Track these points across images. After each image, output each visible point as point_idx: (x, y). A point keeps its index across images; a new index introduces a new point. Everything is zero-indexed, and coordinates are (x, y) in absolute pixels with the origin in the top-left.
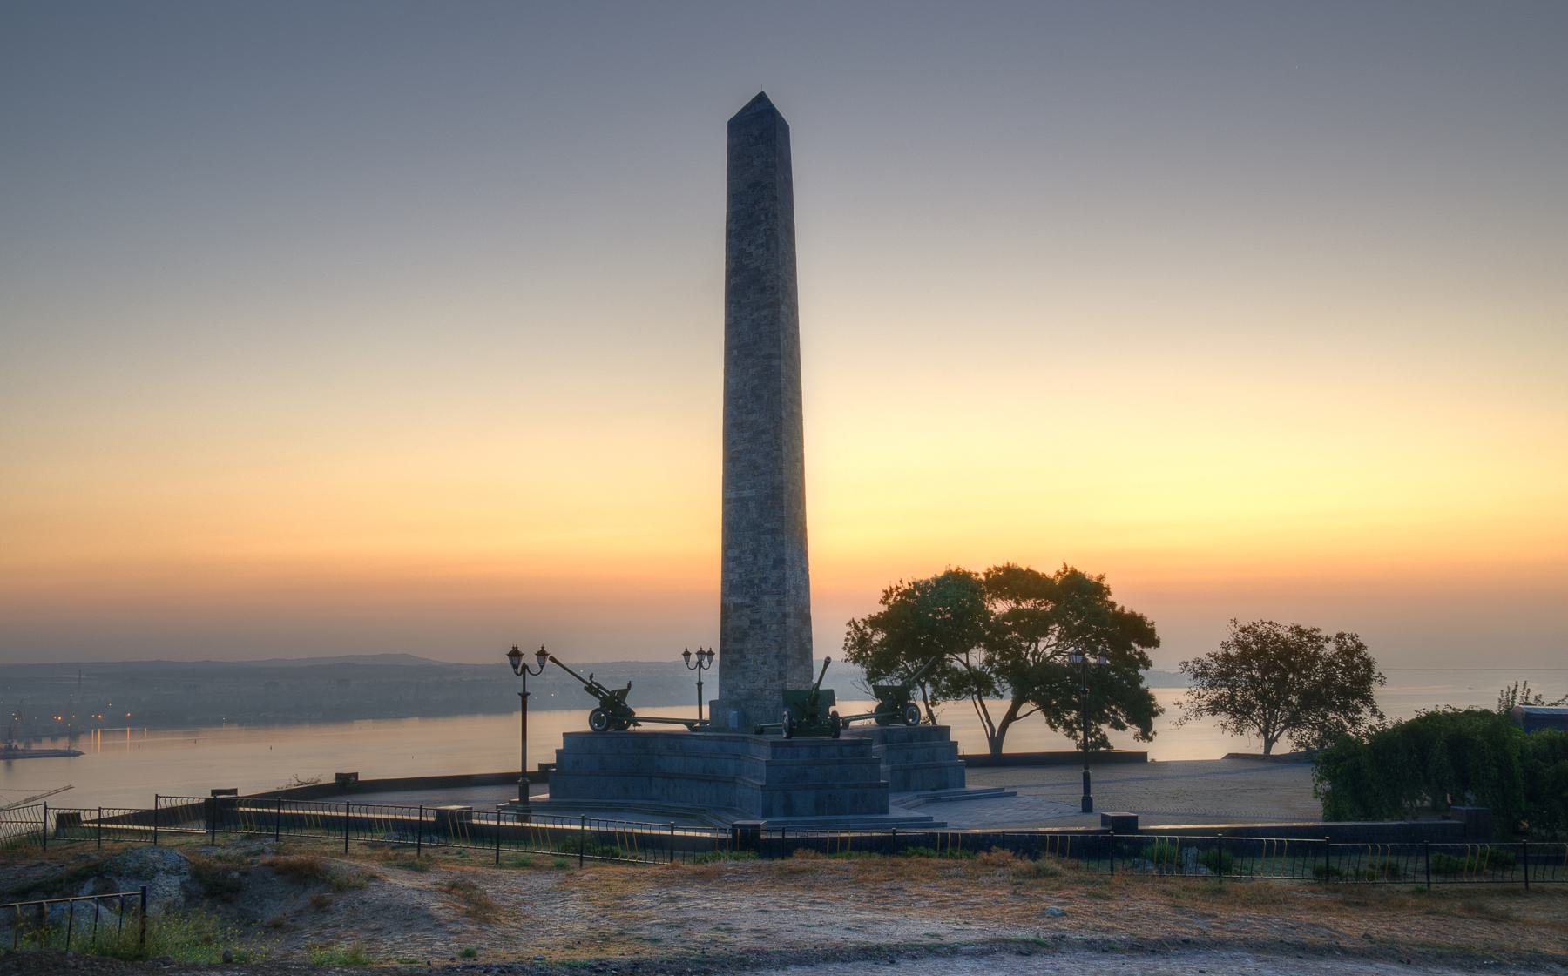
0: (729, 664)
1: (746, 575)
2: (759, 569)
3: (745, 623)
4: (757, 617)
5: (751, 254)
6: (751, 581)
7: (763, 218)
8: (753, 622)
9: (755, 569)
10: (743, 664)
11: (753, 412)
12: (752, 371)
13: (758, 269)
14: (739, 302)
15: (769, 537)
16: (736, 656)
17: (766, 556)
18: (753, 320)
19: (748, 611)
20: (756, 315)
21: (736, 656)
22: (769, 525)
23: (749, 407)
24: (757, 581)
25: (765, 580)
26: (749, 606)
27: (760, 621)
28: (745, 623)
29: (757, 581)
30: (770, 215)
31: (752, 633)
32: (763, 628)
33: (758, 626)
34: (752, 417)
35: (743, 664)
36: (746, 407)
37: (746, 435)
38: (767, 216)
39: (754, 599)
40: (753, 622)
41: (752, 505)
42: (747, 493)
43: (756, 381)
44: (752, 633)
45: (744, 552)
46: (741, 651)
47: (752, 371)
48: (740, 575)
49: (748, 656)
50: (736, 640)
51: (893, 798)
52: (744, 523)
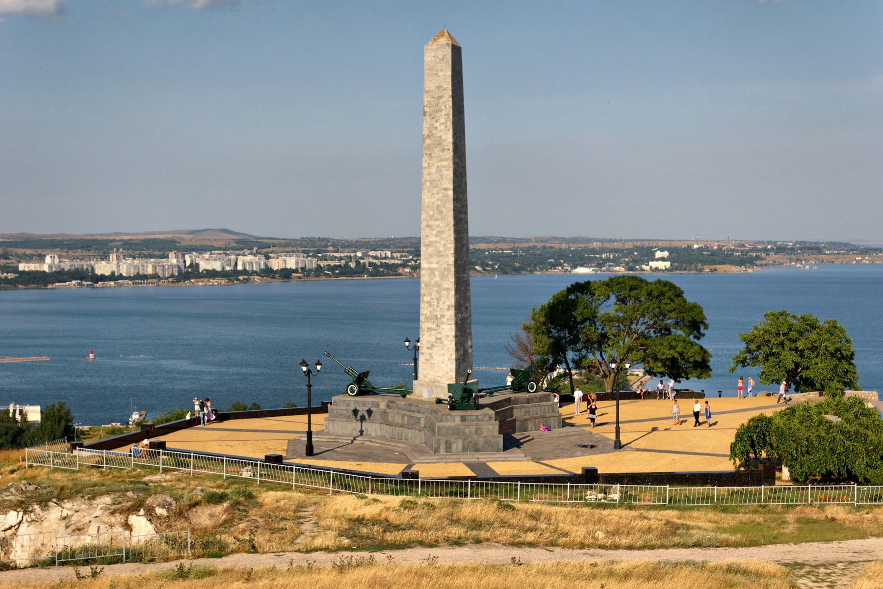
0: (424, 361)
1: (433, 312)
2: (440, 309)
3: (433, 340)
4: (439, 336)
5: (436, 128)
6: (436, 316)
7: (444, 108)
8: (437, 339)
9: (438, 309)
10: (432, 362)
12: (437, 196)
13: (441, 137)
14: (430, 155)
15: (445, 292)
17: (444, 303)
18: (438, 167)
19: (434, 332)
20: (439, 164)
21: (429, 357)
22: (445, 286)
23: (436, 216)
24: (439, 316)
25: (443, 316)
26: (434, 330)
27: (440, 339)
29: (439, 316)
30: (447, 106)
31: (436, 345)
33: (439, 341)
34: (436, 223)
35: (432, 362)
36: (433, 216)
37: (434, 232)
38: (445, 106)
39: (437, 326)
40: (437, 339)
41: (437, 273)
42: (434, 266)
43: (439, 203)
44: (436, 345)
45: (433, 299)
46: (430, 354)
47: (437, 196)
48: (431, 312)
49: (434, 358)
50: (428, 348)
52: (433, 282)
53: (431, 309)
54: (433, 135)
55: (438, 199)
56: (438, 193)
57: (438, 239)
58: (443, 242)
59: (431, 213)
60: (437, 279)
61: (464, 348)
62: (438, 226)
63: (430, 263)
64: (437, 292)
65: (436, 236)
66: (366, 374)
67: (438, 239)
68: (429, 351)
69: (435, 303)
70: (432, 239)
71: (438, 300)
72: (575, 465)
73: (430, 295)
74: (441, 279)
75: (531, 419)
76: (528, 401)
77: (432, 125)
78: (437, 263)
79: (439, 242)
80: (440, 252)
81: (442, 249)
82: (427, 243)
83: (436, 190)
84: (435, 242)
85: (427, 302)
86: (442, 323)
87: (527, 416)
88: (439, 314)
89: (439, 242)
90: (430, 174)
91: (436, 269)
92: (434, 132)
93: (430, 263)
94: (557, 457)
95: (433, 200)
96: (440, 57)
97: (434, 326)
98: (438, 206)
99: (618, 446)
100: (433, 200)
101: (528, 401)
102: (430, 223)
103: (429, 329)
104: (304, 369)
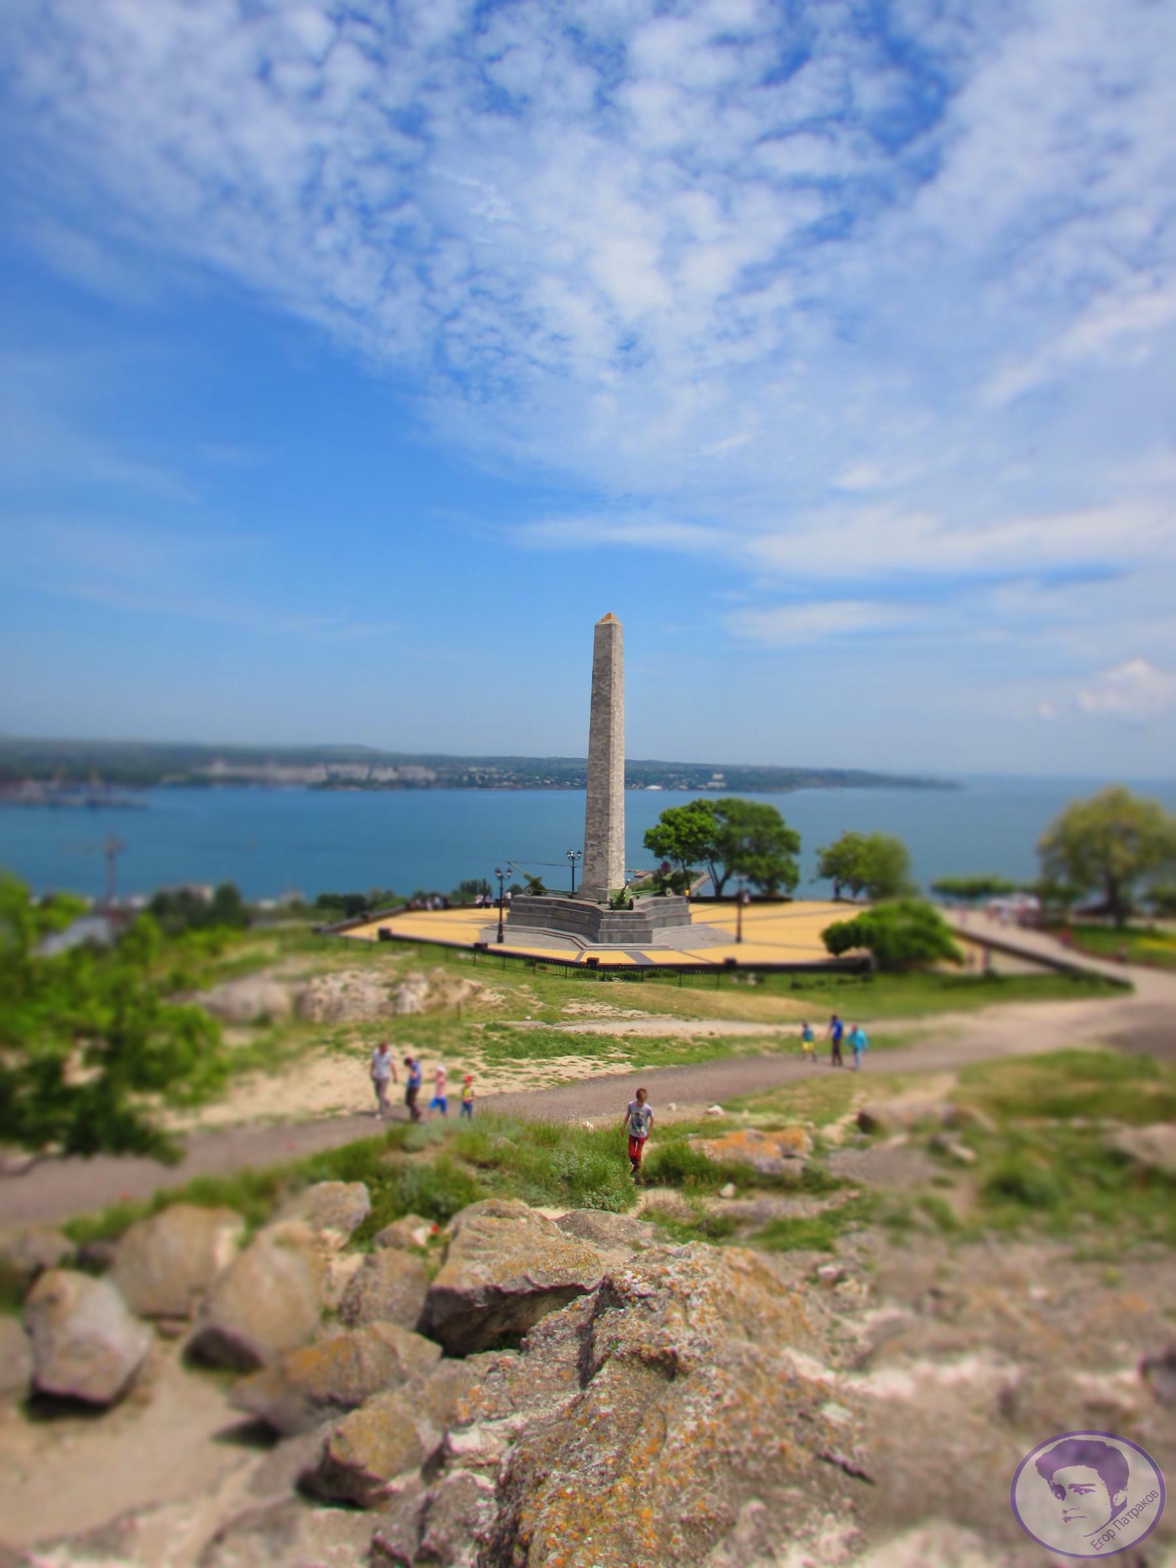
3: (595, 854)
4: (600, 851)
5: (603, 688)
6: (598, 835)
8: (599, 853)
11: (600, 760)
16: (590, 867)
20: (605, 716)
25: (604, 835)
27: (601, 853)
28: (595, 854)
32: (602, 856)
34: (601, 762)
37: (599, 770)
39: (599, 843)
41: (599, 801)
42: (598, 796)
43: (603, 747)
46: (592, 865)
50: (591, 860)
51: (655, 931)
52: (596, 809)
53: (593, 829)
54: (600, 694)
55: (602, 744)
56: (602, 739)
57: (602, 775)
58: (606, 777)
59: (596, 754)
60: (600, 806)
61: (619, 860)
62: (602, 765)
63: (594, 793)
64: (600, 817)
65: (601, 772)
66: (540, 879)
67: (602, 775)
68: (591, 862)
69: (598, 825)
70: (597, 774)
71: (600, 823)
72: (716, 956)
73: (594, 818)
74: (603, 806)
75: (669, 917)
76: (667, 903)
77: (599, 686)
78: (600, 793)
79: (602, 778)
80: (603, 785)
81: (604, 783)
82: (592, 777)
83: (601, 737)
84: (600, 777)
85: (592, 824)
86: (603, 841)
87: (666, 915)
88: (600, 833)
89: (602, 778)
90: (597, 724)
91: (600, 798)
92: (601, 691)
93: (594, 793)
94: (694, 948)
95: (598, 744)
96: (608, 634)
97: (596, 843)
98: (602, 749)
99: (739, 940)
100: (598, 744)
101: (667, 903)
102: (596, 762)
103: (592, 845)
104: (499, 875)
